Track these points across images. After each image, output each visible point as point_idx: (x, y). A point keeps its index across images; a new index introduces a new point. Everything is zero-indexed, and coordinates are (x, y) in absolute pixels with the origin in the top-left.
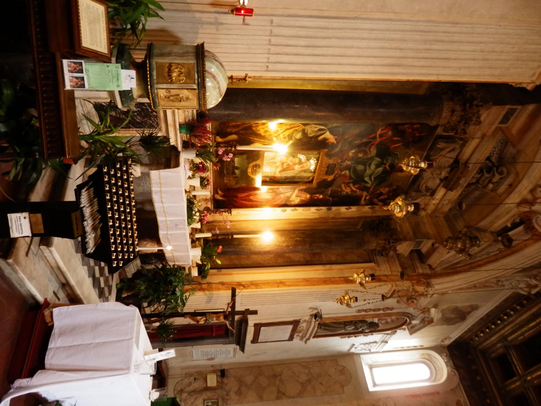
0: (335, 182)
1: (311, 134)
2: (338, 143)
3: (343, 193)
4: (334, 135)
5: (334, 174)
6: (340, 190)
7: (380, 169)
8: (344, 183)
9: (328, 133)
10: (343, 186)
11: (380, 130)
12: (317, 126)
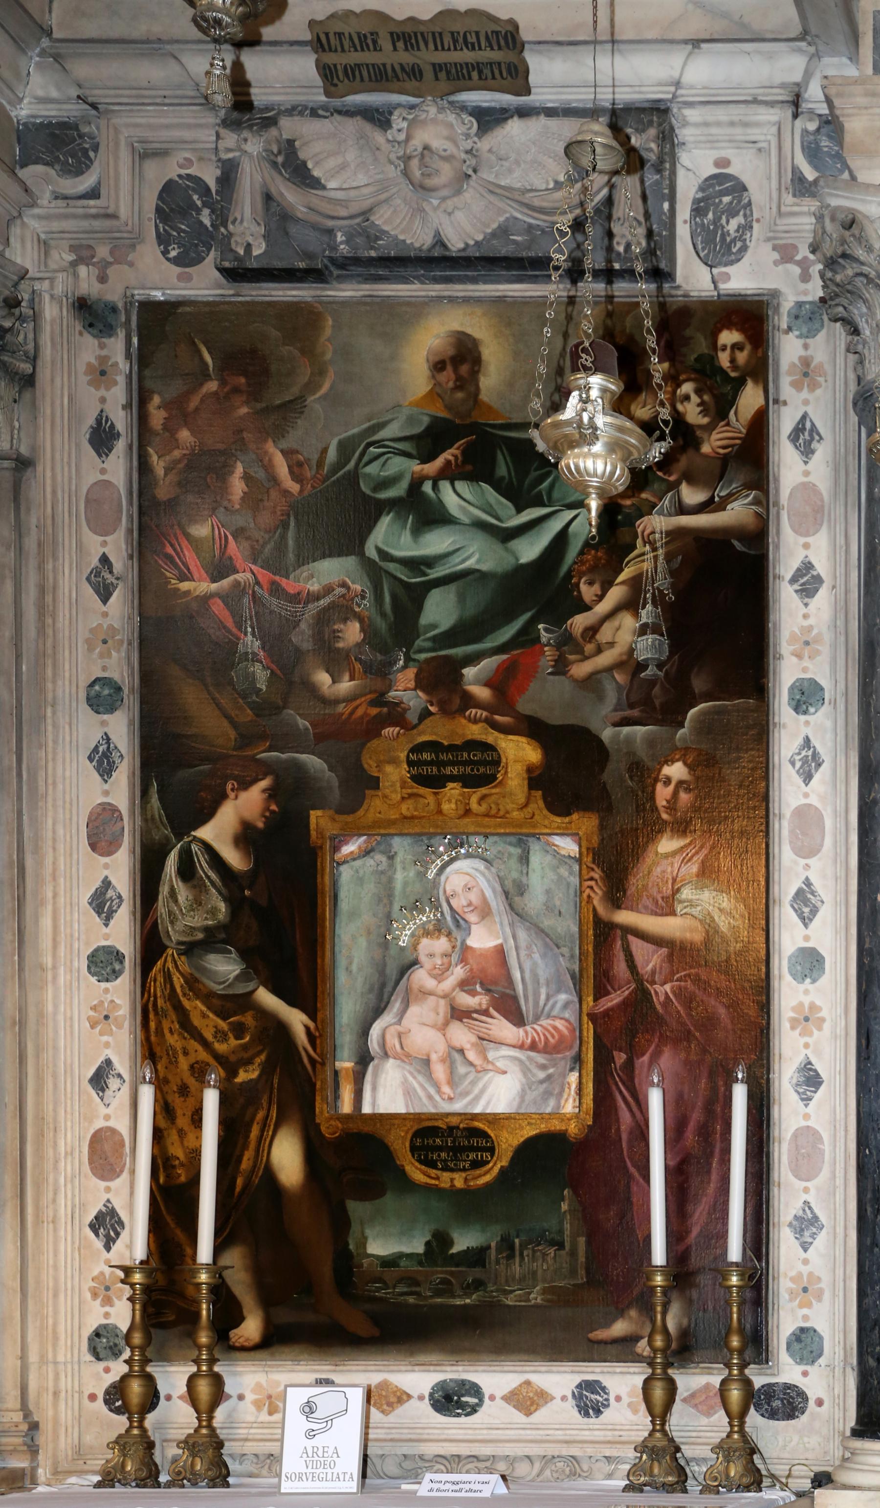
0: (555, 718)
1: (214, 911)
2: (266, 769)
3: (642, 655)
4: (221, 798)
5: (492, 737)
6: (620, 677)
7: (454, 498)
8: (561, 667)
9: (205, 833)
10: (581, 670)
11: (185, 586)
12: (164, 890)
